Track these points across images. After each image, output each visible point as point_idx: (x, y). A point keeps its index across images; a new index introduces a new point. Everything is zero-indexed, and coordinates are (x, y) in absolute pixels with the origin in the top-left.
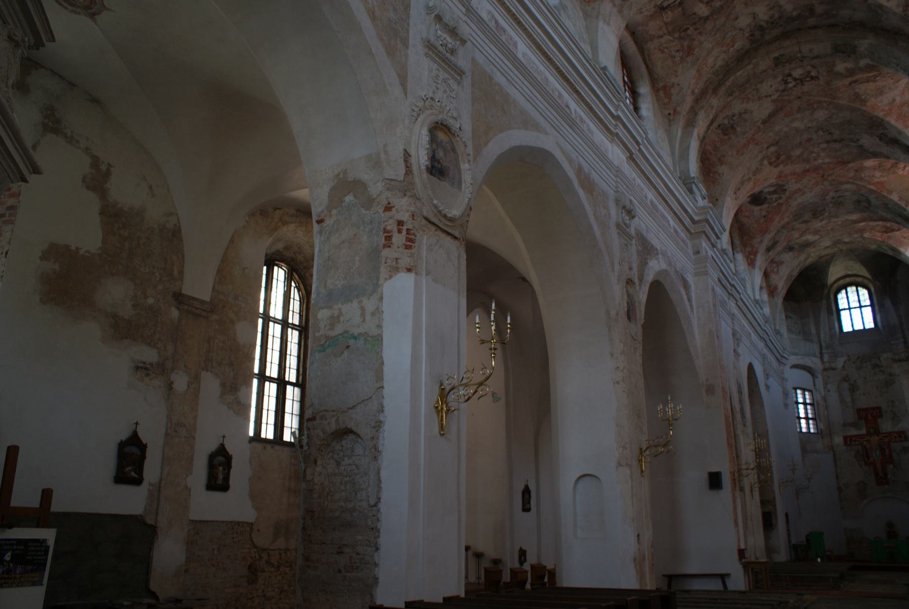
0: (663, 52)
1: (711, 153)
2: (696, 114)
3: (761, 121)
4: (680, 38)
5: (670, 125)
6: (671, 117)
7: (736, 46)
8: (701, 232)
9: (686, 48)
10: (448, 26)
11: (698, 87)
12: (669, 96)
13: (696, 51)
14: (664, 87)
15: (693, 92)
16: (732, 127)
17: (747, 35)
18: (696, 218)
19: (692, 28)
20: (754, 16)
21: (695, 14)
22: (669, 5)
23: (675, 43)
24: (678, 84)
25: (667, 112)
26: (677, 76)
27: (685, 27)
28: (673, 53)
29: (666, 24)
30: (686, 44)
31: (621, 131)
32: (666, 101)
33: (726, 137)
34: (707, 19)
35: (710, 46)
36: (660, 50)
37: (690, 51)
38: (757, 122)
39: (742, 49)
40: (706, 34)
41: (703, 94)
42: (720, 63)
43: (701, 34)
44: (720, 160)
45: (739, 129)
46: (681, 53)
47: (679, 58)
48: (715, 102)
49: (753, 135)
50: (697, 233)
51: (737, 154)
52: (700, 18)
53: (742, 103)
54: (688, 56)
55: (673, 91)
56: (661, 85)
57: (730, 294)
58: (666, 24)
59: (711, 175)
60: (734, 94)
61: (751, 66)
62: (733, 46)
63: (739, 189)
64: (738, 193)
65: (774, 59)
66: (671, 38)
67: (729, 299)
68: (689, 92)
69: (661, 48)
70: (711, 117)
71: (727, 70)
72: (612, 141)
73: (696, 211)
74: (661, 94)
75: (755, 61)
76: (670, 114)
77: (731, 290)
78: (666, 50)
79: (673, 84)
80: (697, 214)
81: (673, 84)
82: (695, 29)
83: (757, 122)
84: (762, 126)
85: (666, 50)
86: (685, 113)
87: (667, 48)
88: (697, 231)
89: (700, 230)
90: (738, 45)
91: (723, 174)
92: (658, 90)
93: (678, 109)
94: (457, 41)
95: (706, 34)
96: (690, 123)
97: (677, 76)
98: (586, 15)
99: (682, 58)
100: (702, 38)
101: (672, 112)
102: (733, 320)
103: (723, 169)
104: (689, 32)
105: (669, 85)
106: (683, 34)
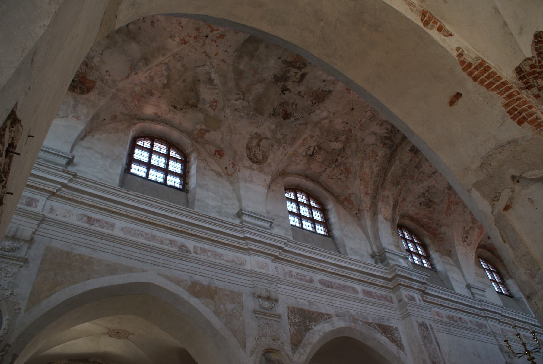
0: (333, 179)
1: (429, 223)
2: (377, 206)
3: (446, 190)
4: (337, 166)
5: (360, 220)
6: (358, 215)
7: (379, 155)
8: (397, 285)
9: (344, 171)
10: (9, 236)
11: (369, 189)
12: (350, 202)
13: (351, 169)
14: (345, 199)
15: (367, 194)
16: (430, 201)
17: (381, 145)
18: (390, 277)
19: (339, 158)
20: (375, 134)
21: (334, 149)
22: (313, 152)
23: (336, 171)
24: (353, 193)
25: (354, 213)
26: (349, 189)
27: (335, 159)
28: (339, 177)
29: (322, 163)
30: (342, 168)
31: (253, 246)
32: (351, 206)
33: (431, 209)
34: (344, 149)
35: (359, 162)
36: (330, 178)
37: (348, 171)
38: (444, 190)
39: (386, 154)
40: (350, 157)
41: (376, 191)
42: (376, 170)
43: (347, 158)
44: (437, 224)
45: (435, 200)
46: (343, 174)
47: (344, 178)
48: (387, 193)
49: (449, 199)
50: (395, 286)
51: (447, 216)
52: (340, 150)
53: (418, 184)
54: (349, 174)
55: (352, 199)
56: (343, 198)
57: (486, 317)
58: (322, 163)
59: (438, 236)
60: (401, 182)
61: (397, 162)
62: (378, 156)
63: (467, 237)
64: (467, 240)
65: (410, 150)
66: (332, 169)
67: (487, 321)
68: (363, 195)
69: (330, 177)
70: (392, 203)
71: (384, 171)
72: (250, 254)
73: (388, 271)
74: (345, 203)
75: (397, 158)
76: (356, 213)
77: (485, 314)
78: (333, 177)
79: (350, 194)
80: (389, 274)
81: (350, 194)
82: (342, 157)
83: (444, 190)
84: (450, 192)
85: (333, 177)
86: (368, 208)
87: (333, 175)
88: (394, 285)
89: (396, 284)
90: (381, 154)
91: (446, 233)
92: (343, 202)
93: (360, 208)
94: (21, 242)
95: (350, 157)
96: (375, 214)
97: (349, 189)
98: (232, 183)
99: (346, 177)
100: (350, 160)
101: (357, 212)
102: (495, 337)
103: (443, 229)
104: (340, 160)
105: (347, 196)
106: (336, 163)
